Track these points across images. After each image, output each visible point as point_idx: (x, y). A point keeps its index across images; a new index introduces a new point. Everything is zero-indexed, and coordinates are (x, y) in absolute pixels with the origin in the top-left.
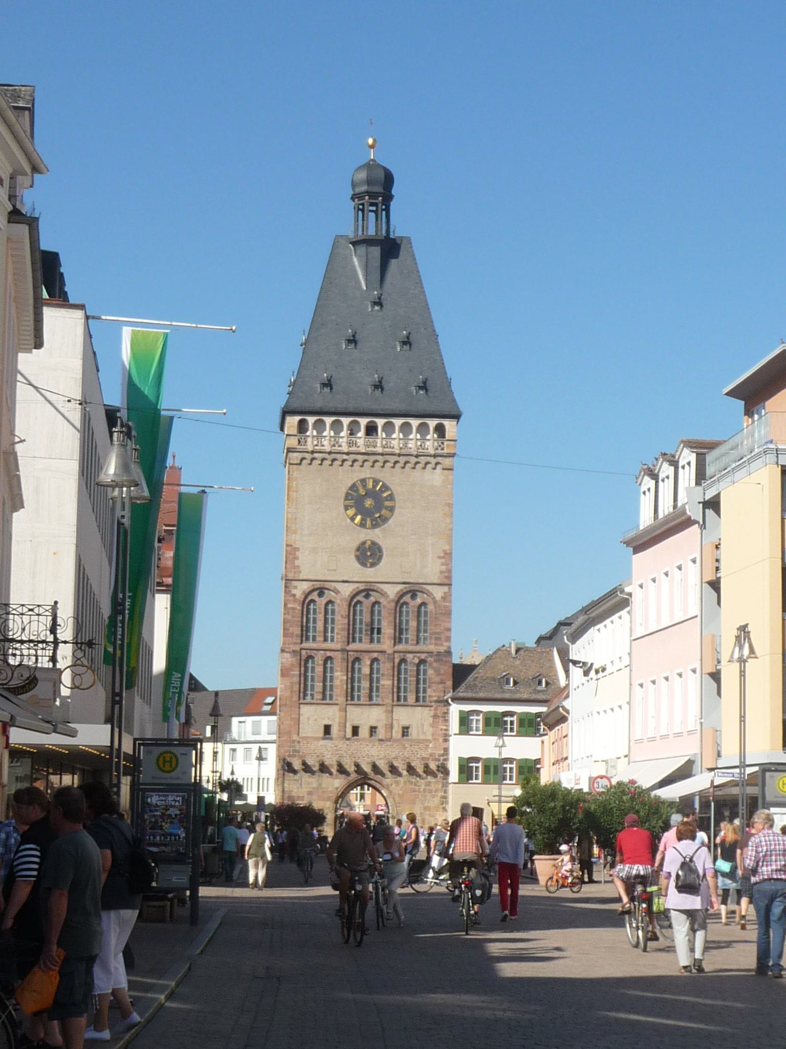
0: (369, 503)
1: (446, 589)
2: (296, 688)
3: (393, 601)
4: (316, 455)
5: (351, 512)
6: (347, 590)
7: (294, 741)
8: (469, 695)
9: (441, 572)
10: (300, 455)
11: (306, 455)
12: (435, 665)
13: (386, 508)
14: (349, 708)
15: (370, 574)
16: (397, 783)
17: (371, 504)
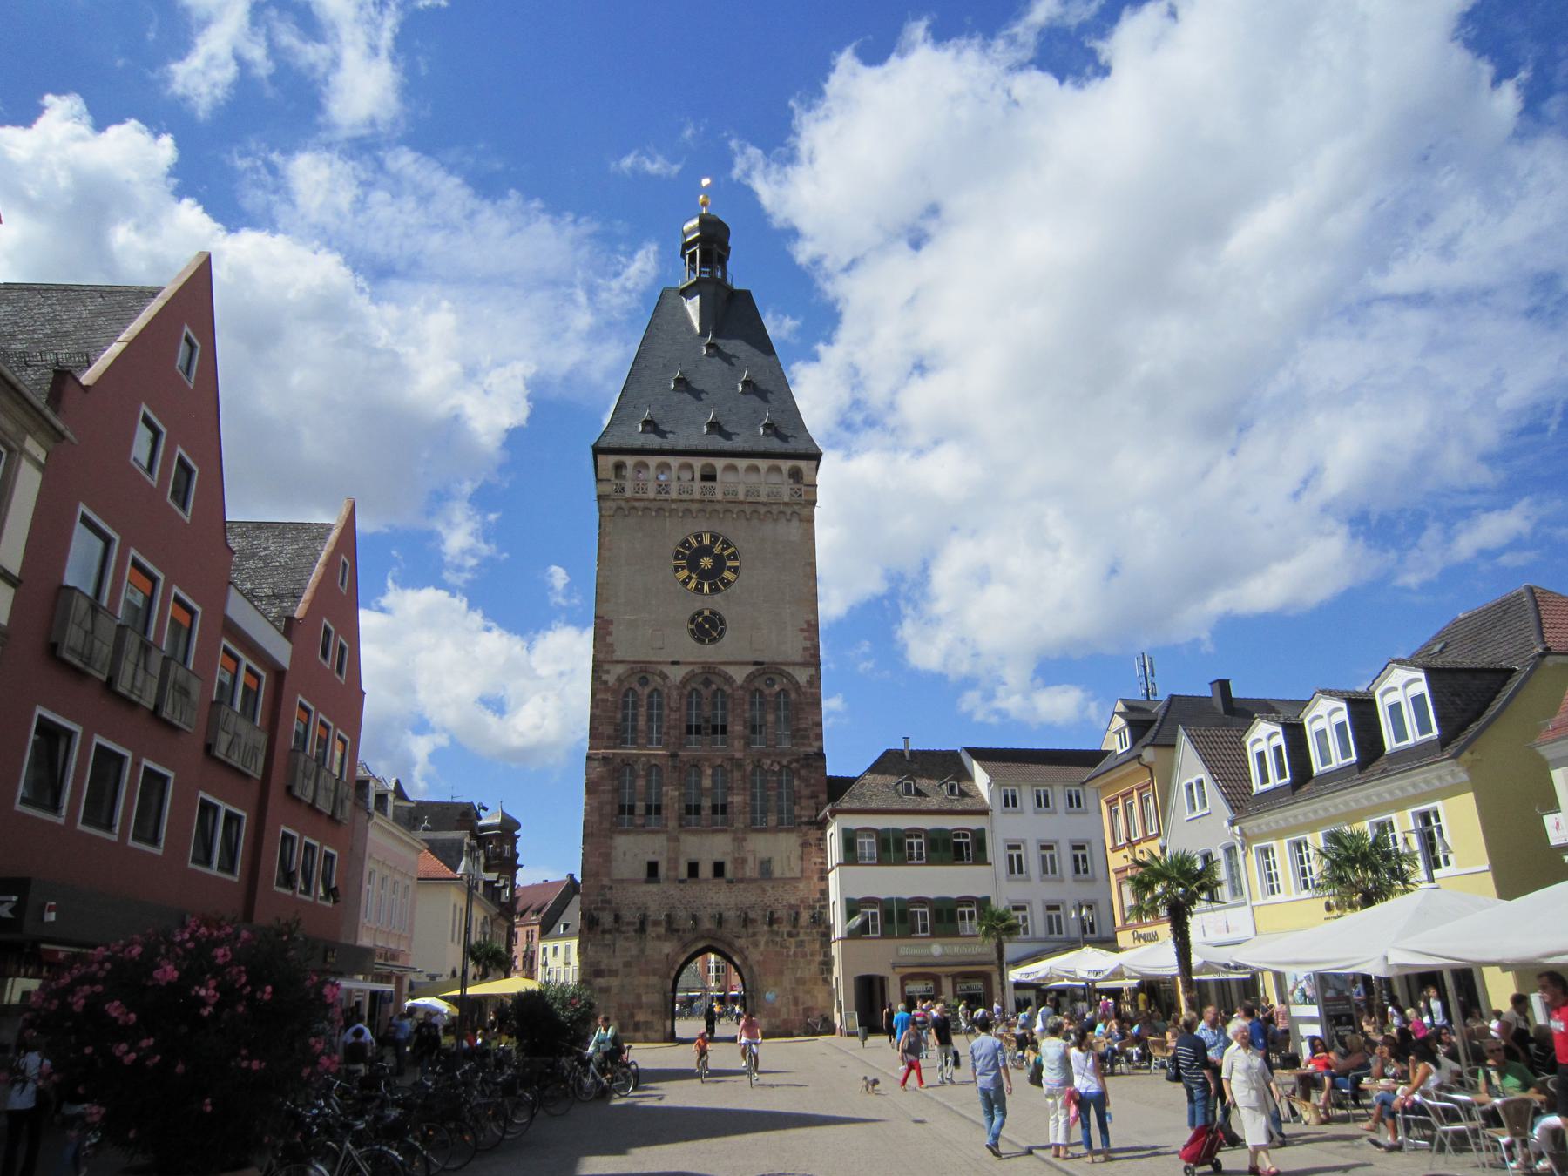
0: (706, 563)
1: (812, 671)
2: (607, 809)
3: (741, 687)
4: (636, 504)
5: (684, 574)
6: (676, 674)
7: (603, 887)
8: (856, 805)
9: (805, 649)
10: (613, 505)
11: (623, 504)
12: (803, 772)
13: (729, 569)
14: (683, 837)
15: (709, 653)
16: (756, 945)
17: (707, 564)
